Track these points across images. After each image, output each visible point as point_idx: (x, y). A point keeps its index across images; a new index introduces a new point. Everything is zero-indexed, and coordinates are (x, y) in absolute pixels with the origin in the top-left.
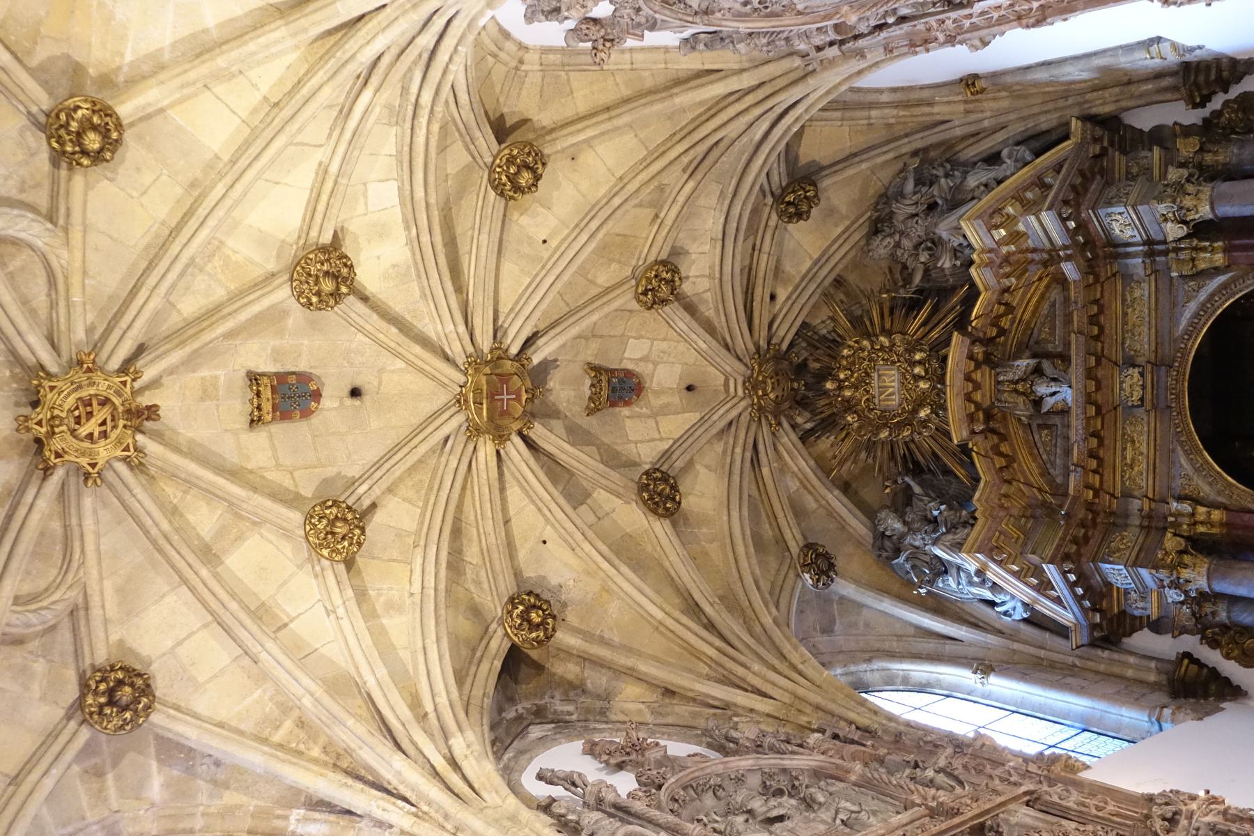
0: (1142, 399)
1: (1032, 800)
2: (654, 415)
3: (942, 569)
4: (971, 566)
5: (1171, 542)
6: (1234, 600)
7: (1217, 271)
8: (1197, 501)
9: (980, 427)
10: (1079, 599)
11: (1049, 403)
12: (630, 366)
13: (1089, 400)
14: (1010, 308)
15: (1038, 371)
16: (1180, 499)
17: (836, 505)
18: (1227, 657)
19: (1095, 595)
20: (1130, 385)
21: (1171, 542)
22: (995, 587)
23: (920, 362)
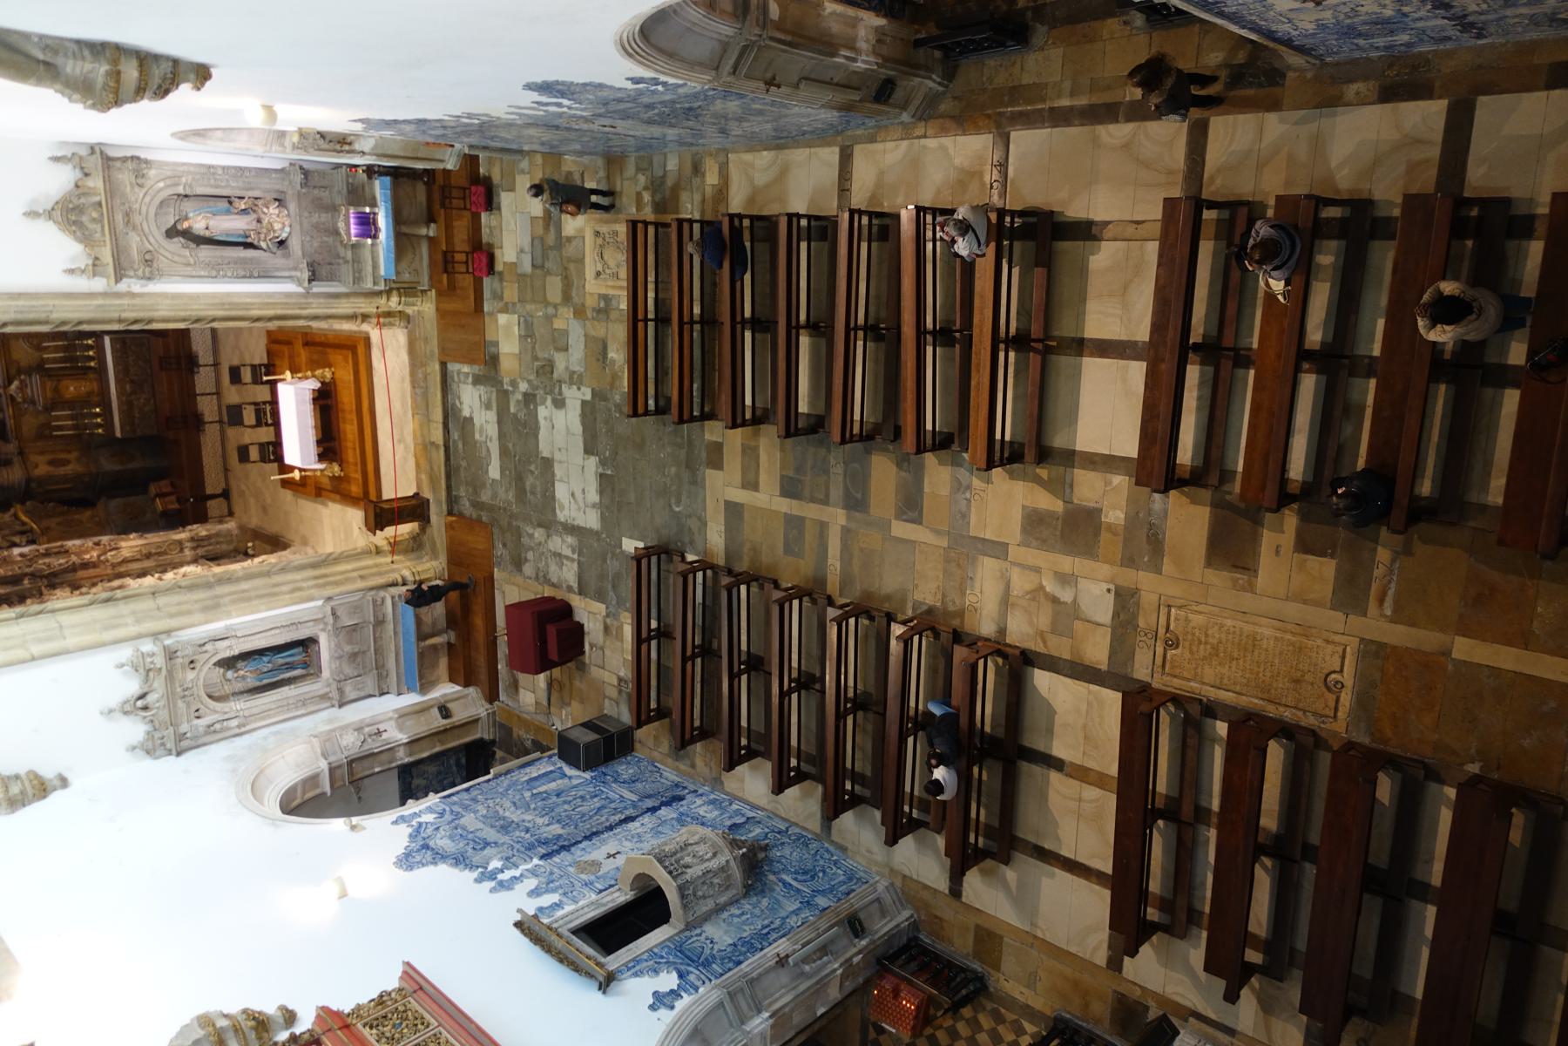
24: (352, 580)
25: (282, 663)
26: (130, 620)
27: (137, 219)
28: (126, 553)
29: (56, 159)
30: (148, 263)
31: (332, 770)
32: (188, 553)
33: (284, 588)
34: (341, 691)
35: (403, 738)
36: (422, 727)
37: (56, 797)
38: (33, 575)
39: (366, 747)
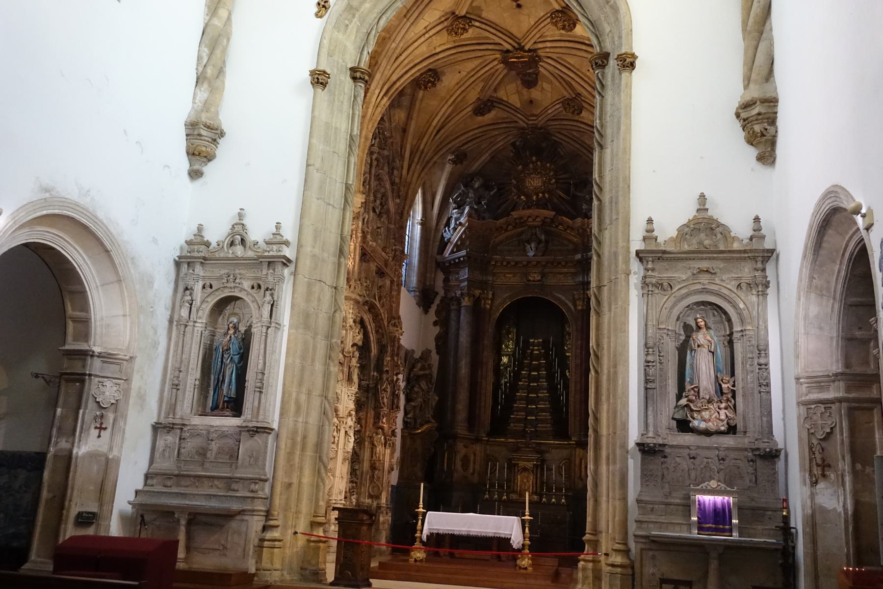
0: (529, 280)
1: (392, 282)
2: (518, 92)
3: (460, 206)
4: (463, 220)
5: (477, 292)
6: (459, 311)
7: (575, 306)
8: (492, 300)
9: (517, 221)
10: (454, 260)
11: (529, 246)
12: (539, 83)
13: (529, 262)
14: (565, 230)
15: (540, 242)
16: (493, 294)
17: (483, 158)
18: (438, 306)
19: (457, 265)
20: (535, 276)
21: (477, 292)
22: (455, 229)
23: (544, 196)
24: (289, 472)
25: (225, 378)
26: (317, 251)
27: (704, 279)
28: (379, 449)
29: (757, 219)
30: (659, 285)
31: (84, 355)
32: (368, 501)
33: (303, 397)
34: (169, 428)
35: (81, 450)
36: (82, 479)
37: (183, 163)
38: (381, 379)
39: (91, 404)
